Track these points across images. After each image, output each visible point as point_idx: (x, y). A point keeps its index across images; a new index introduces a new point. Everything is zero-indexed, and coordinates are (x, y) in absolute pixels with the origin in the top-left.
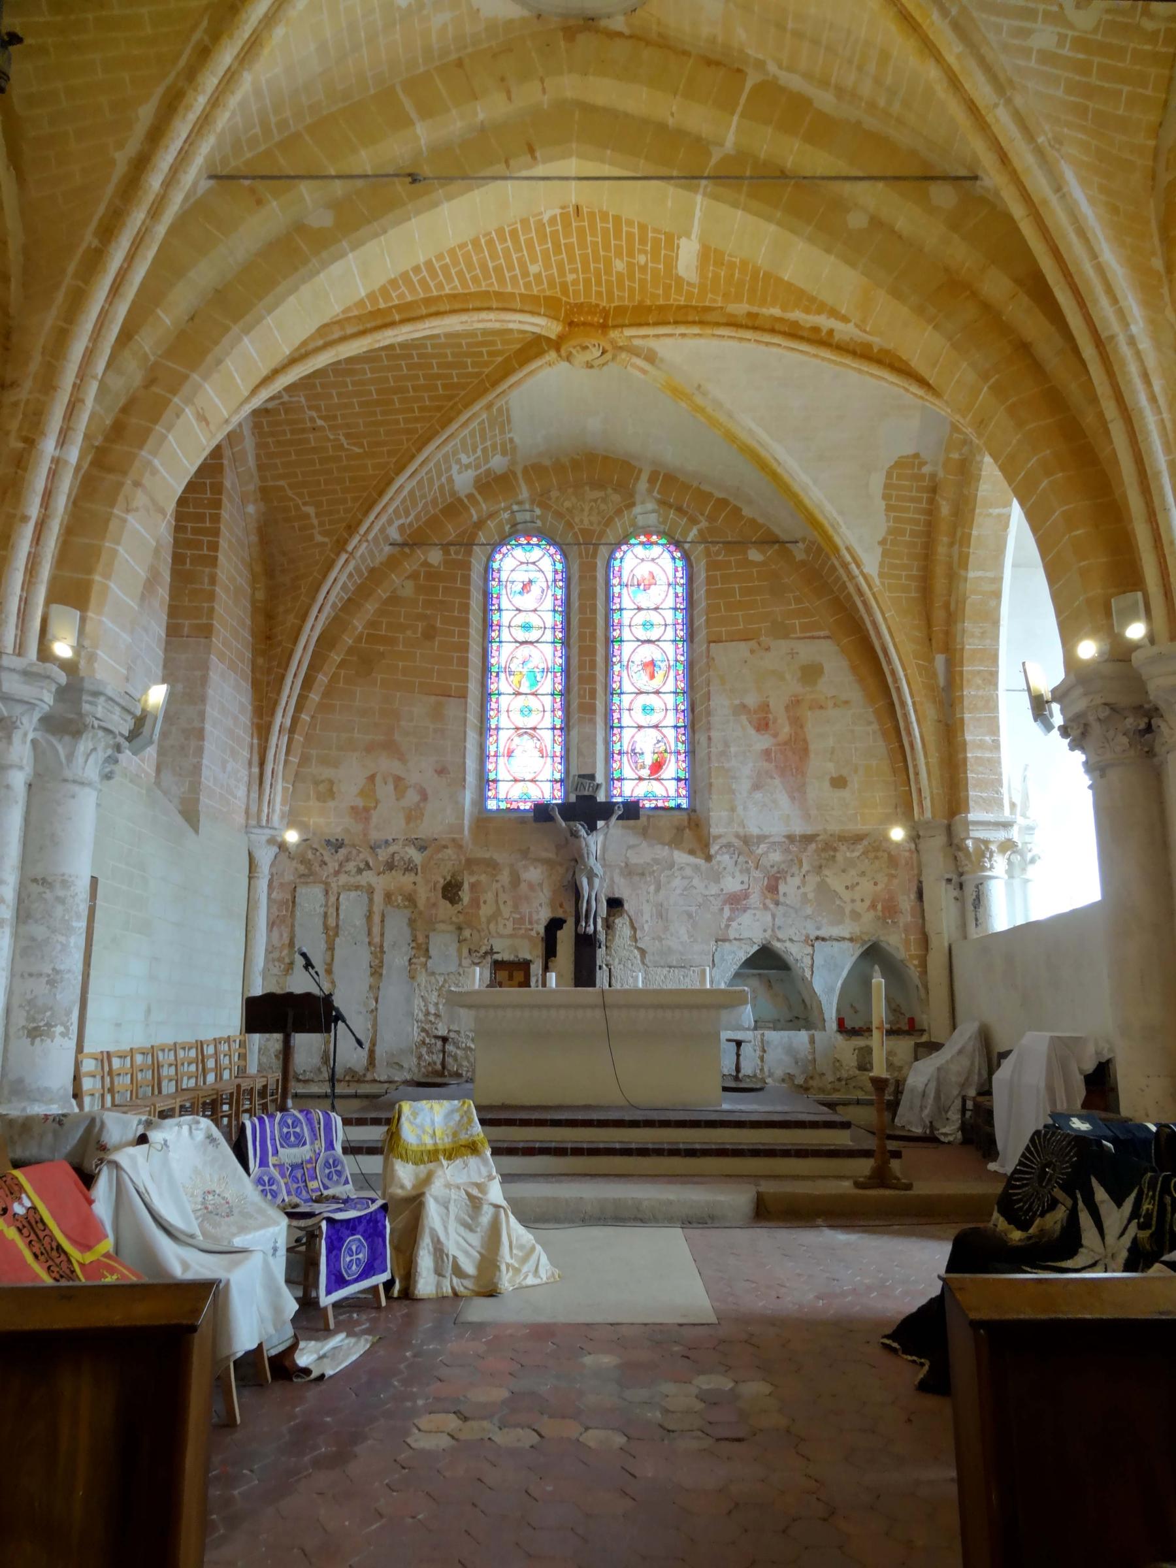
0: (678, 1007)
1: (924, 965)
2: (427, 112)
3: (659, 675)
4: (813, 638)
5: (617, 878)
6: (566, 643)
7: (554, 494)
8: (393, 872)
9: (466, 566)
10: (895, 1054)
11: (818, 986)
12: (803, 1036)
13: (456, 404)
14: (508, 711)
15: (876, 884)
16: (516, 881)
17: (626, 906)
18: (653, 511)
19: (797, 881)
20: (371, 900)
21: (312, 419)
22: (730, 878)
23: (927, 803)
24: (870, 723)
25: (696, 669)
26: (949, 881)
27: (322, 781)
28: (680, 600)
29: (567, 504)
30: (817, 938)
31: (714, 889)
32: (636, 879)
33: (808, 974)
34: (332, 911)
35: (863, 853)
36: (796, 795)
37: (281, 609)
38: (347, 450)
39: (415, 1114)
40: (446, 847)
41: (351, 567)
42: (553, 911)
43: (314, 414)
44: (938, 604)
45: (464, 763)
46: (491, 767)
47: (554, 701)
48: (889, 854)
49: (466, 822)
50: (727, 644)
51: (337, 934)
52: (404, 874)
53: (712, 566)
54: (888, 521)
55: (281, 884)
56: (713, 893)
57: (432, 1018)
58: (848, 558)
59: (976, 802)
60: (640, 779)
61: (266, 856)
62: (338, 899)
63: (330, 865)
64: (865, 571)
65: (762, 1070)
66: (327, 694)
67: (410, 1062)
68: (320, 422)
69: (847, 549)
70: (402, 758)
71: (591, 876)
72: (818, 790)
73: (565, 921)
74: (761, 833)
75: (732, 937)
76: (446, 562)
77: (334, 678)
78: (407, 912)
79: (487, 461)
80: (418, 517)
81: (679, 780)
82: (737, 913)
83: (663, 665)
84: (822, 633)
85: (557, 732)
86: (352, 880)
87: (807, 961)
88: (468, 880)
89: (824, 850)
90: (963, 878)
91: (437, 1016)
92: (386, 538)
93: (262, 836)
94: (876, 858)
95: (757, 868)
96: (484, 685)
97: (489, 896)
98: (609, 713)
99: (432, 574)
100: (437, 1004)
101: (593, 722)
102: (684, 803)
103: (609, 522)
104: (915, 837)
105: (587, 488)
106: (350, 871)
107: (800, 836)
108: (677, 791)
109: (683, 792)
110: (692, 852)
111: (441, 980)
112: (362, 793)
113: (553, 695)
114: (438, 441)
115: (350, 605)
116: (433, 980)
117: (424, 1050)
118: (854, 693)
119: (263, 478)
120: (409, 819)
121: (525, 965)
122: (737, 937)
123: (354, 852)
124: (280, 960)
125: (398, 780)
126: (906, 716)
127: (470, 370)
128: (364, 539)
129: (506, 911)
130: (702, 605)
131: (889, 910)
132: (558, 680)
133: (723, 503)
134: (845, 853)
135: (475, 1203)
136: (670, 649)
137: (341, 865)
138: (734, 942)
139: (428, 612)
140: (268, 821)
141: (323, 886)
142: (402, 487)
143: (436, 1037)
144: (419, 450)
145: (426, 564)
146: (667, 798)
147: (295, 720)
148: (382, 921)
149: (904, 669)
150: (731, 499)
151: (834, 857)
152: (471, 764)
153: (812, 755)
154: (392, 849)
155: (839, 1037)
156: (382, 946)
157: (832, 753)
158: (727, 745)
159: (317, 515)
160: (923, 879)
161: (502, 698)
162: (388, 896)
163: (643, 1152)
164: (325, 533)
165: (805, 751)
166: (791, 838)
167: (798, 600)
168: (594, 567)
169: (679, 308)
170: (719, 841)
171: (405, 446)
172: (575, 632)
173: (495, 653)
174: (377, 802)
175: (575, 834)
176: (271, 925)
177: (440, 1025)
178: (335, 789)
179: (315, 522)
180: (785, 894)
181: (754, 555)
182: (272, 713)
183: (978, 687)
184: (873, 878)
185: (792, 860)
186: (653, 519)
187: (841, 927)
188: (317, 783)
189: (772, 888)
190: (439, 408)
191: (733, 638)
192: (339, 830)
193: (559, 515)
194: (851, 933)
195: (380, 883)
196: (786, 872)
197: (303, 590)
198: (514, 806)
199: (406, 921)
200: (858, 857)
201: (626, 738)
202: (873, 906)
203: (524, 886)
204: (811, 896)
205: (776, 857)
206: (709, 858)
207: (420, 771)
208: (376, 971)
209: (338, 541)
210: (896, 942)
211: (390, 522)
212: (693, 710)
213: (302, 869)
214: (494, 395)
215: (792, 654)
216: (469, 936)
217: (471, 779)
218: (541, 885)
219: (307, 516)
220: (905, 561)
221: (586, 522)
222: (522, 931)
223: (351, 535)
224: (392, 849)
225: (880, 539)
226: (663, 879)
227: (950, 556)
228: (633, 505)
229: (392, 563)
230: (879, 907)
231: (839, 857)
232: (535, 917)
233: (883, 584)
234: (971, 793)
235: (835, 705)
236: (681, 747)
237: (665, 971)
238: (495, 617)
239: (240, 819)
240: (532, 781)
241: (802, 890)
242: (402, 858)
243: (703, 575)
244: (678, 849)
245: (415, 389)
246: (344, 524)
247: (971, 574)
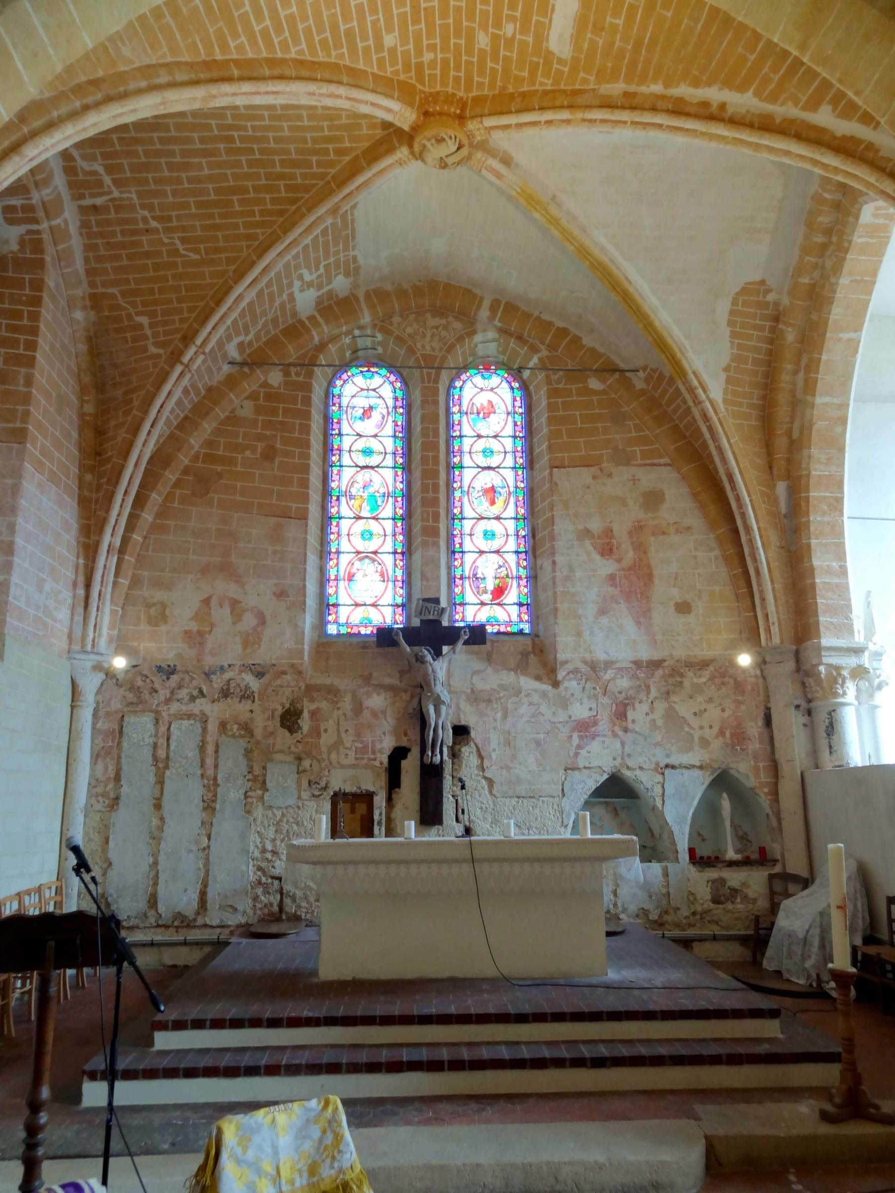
0: (552, 860)
1: (775, 792)
3: (500, 501)
4: (654, 465)
5: (463, 704)
6: (407, 468)
7: (396, 319)
8: (229, 699)
9: (307, 387)
10: (748, 886)
11: (670, 814)
12: (656, 868)
13: (299, 208)
14: (348, 535)
15: (723, 710)
16: (358, 709)
17: (473, 734)
18: (494, 340)
19: (645, 707)
20: (205, 729)
21: (145, 220)
22: (578, 704)
23: (775, 629)
24: (711, 550)
25: (538, 495)
26: (797, 707)
27: (154, 604)
28: (518, 428)
29: (409, 330)
30: (667, 766)
31: (562, 716)
32: (482, 705)
33: (659, 803)
34: (162, 741)
35: (710, 679)
36: (641, 620)
37: (113, 423)
38: (185, 256)
39: (245, 1140)
40: (284, 673)
41: (185, 381)
42: (396, 741)
43: (146, 213)
44: (780, 430)
45: (305, 586)
46: (331, 591)
47: (395, 526)
48: (735, 679)
49: (306, 647)
50: (570, 469)
51: (167, 767)
52: (240, 701)
53: (553, 393)
54: (732, 348)
55: (108, 713)
56: (561, 720)
57: (269, 856)
58: (695, 383)
59: (827, 628)
60: (483, 604)
61: (90, 684)
62: (169, 729)
63: (161, 692)
64: (711, 396)
65: (615, 905)
66: (159, 515)
67: (245, 904)
68: (154, 224)
69: (694, 373)
70: (239, 581)
71: (438, 703)
73: (409, 750)
74: (607, 658)
75: (581, 765)
76: (286, 383)
77: (169, 497)
78: (243, 743)
79: (329, 282)
80: (257, 336)
81: (520, 605)
82: (585, 740)
83: (504, 491)
84: (662, 461)
85: (399, 557)
86: (184, 708)
87: (658, 790)
88: (308, 707)
89: (671, 676)
90: (812, 705)
91: (274, 853)
92: (225, 355)
93: (87, 662)
94: (723, 684)
95: (605, 694)
96: (324, 508)
97: (330, 724)
98: (451, 537)
99: (272, 396)
100: (274, 840)
101: (436, 545)
102: (526, 628)
103: (450, 349)
104: (762, 663)
105: (428, 315)
106: (183, 699)
107: (647, 662)
108: (519, 616)
109: (525, 617)
110: (538, 678)
111: (279, 814)
112: (196, 617)
113: (394, 519)
114: (279, 248)
115: (187, 424)
116: (270, 813)
117: (260, 891)
119: (92, 285)
120: (246, 644)
121: (368, 798)
122: (587, 765)
123: (187, 678)
124: (104, 795)
125: (234, 603)
126: (751, 541)
127: (315, 170)
128: (201, 350)
129: (348, 740)
131: (738, 738)
132: (399, 504)
133: (563, 332)
134: (691, 679)
136: (510, 475)
137: (172, 692)
138: (584, 771)
139: (268, 433)
140: (93, 646)
141: (153, 715)
142: (240, 298)
143: (273, 878)
144: (260, 257)
145: (265, 385)
146: (509, 623)
147: (125, 540)
148: (217, 752)
149: (749, 495)
150: (571, 329)
151: (681, 682)
152: (311, 588)
153: (656, 581)
154: (227, 675)
155: (693, 869)
156: (215, 779)
157: (676, 579)
158: (571, 569)
159: (151, 326)
160: (772, 705)
161: (343, 522)
162: (223, 725)
164: (162, 345)
165: (650, 576)
166: (637, 664)
167: (637, 428)
168: (436, 392)
169: (546, 93)
170: (566, 666)
171: (245, 254)
173: (335, 477)
174: (212, 626)
175: (420, 660)
176: (96, 757)
177: (278, 863)
178: (167, 612)
179: (149, 333)
180: (633, 721)
181: (594, 384)
182: (101, 531)
183: (824, 514)
185: (640, 686)
186: (492, 349)
187: (690, 754)
188: (149, 606)
189: (621, 714)
190: (282, 213)
191: (576, 464)
192: (171, 655)
193: (400, 340)
194: (700, 761)
195: (214, 711)
196: (634, 698)
197: (136, 403)
198: (355, 630)
199: (242, 751)
200: (705, 683)
202: (722, 733)
203: (366, 715)
204: (660, 723)
205: (624, 683)
206: (556, 684)
208: (209, 807)
209: (173, 353)
211: (229, 338)
212: (534, 536)
213: (130, 697)
214: (341, 196)
215: (634, 480)
216: (308, 768)
217: (311, 602)
218: (384, 712)
219: (140, 326)
220: (747, 389)
221: (428, 347)
222: (365, 762)
223: (187, 346)
224: (227, 675)
225: (724, 365)
226: (510, 706)
227: (794, 384)
228: (473, 333)
229: (231, 382)
230: (728, 734)
231: (686, 683)
232: (378, 746)
233: (727, 410)
234: (822, 619)
235: (678, 531)
236: (523, 573)
237: (514, 801)
238: (336, 442)
239: (61, 644)
240: (374, 605)
241: (651, 717)
242: (239, 685)
243: (544, 403)
244: (524, 675)
245: (256, 189)
246: (179, 336)
247: (819, 400)
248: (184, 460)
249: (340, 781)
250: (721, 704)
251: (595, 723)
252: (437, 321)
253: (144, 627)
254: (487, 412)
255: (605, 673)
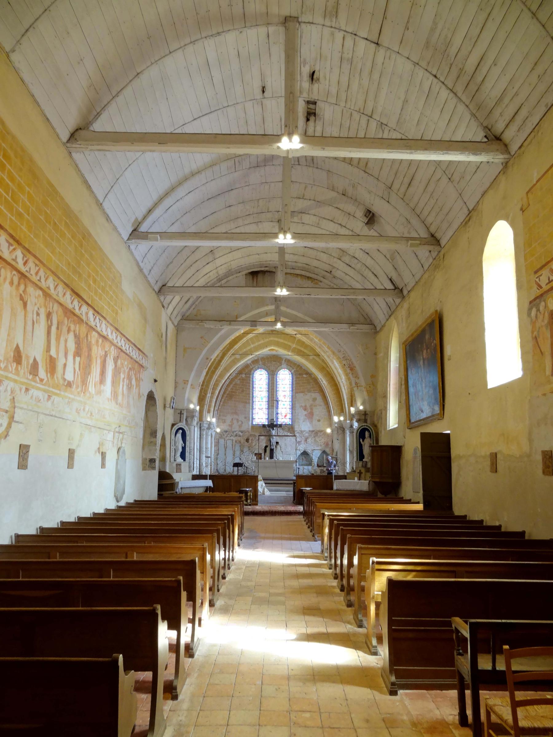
2: (253, 344)
3: (286, 398)
6: (268, 391)
7: (266, 363)
9: (250, 377)
12: (310, 467)
19: (311, 439)
34: (226, 444)
46: (254, 416)
61: (214, 434)
72: (315, 422)
76: (246, 377)
78: (239, 444)
88: (250, 438)
99: (243, 379)
101: (273, 408)
104: (332, 431)
112: (231, 422)
118: (322, 404)
121: (261, 454)
125: (237, 419)
130: (294, 386)
131: (327, 445)
133: (299, 365)
134: (319, 434)
135: (262, 486)
145: (242, 377)
152: (251, 416)
154: (237, 432)
162: (236, 441)
163: (281, 484)
165: (313, 414)
166: (310, 431)
172: (270, 391)
175: (270, 431)
176: (215, 446)
181: (305, 376)
189: (306, 440)
195: (235, 439)
201: (280, 411)
202: (324, 444)
205: (307, 435)
207: (241, 418)
208: (234, 455)
210: (328, 450)
217: (251, 419)
224: (237, 432)
229: (236, 377)
236: (290, 412)
238: (255, 386)
248: (227, 392)
249: (256, 452)
251: (301, 441)
252: (274, 363)
253: (222, 424)
254: (283, 380)
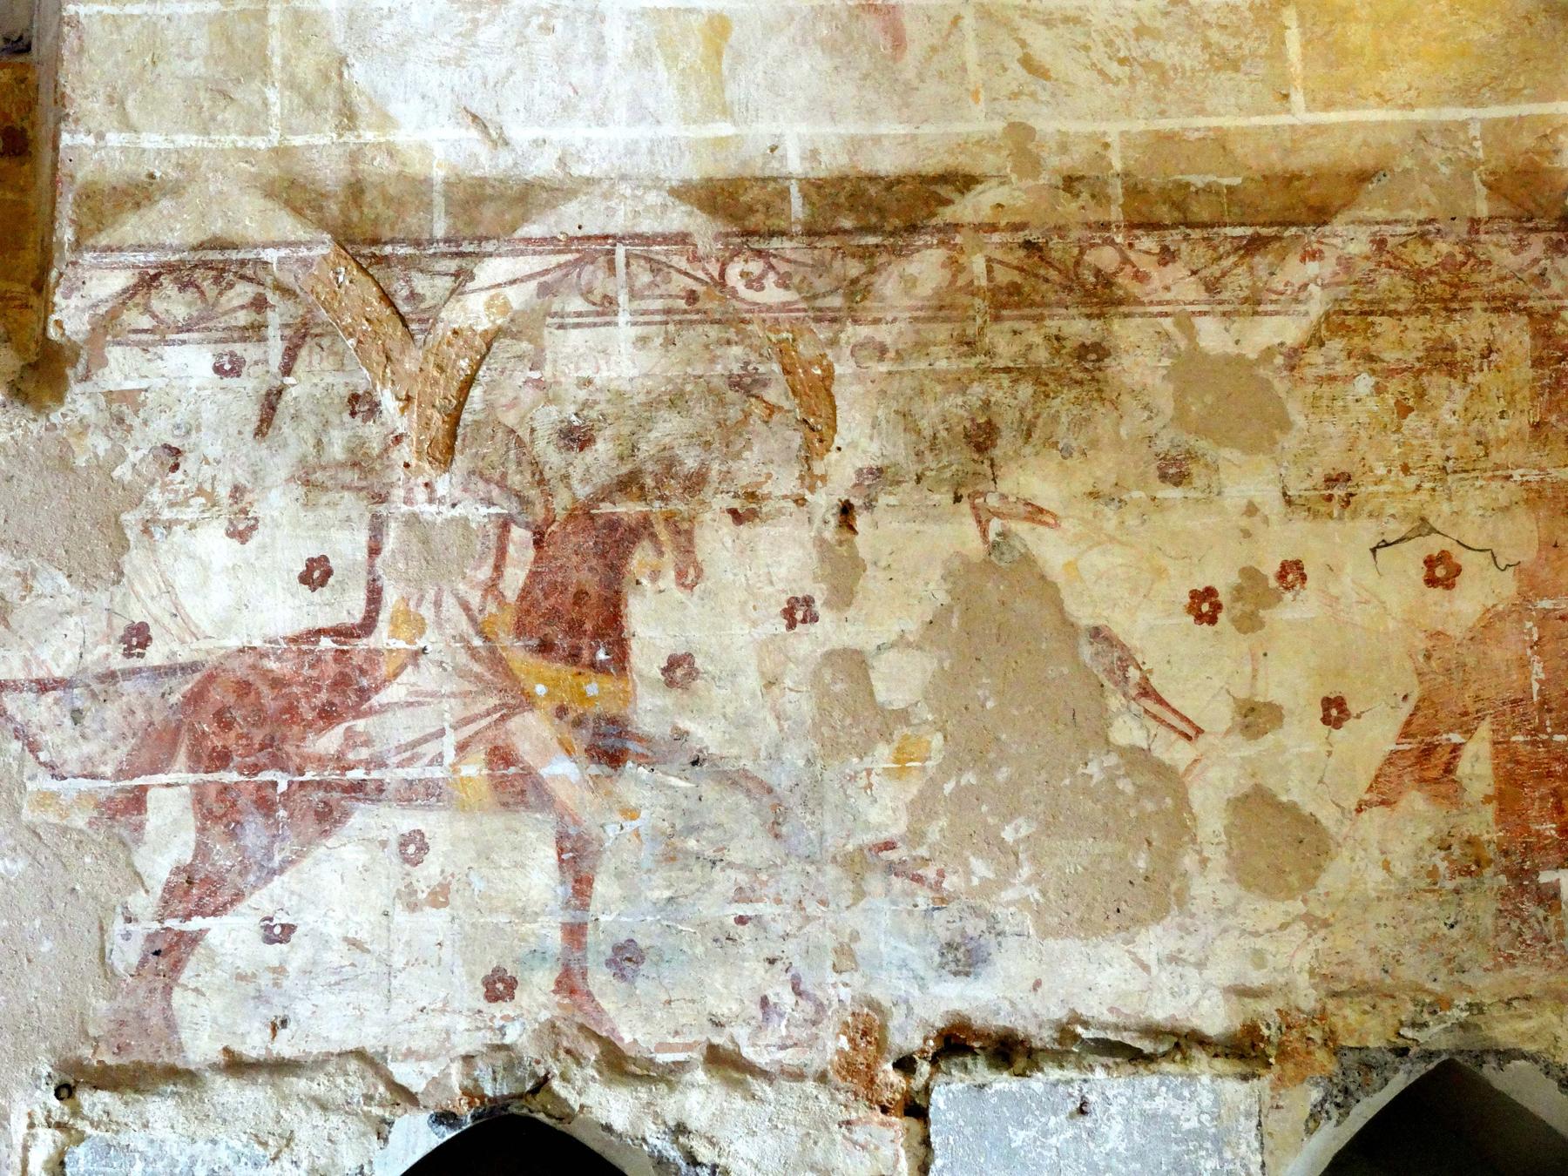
22: (213, 540)
35: (1335, 323)
56: (58, 659)
74: (488, 163)
75: (201, 1048)
82: (254, 832)
94: (1442, 359)
95: (444, 451)
107: (816, 188)
122: (254, 1045)
138: (226, 1091)
151: (1094, 353)
170: (132, 227)
180: (678, 670)
184: (1424, 527)
185: (746, 385)
187: (1154, 941)
196: (695, 483)
200: (1294, 358)
241: (829, 631)
250: (1424, 527)
255: (462, 277)
